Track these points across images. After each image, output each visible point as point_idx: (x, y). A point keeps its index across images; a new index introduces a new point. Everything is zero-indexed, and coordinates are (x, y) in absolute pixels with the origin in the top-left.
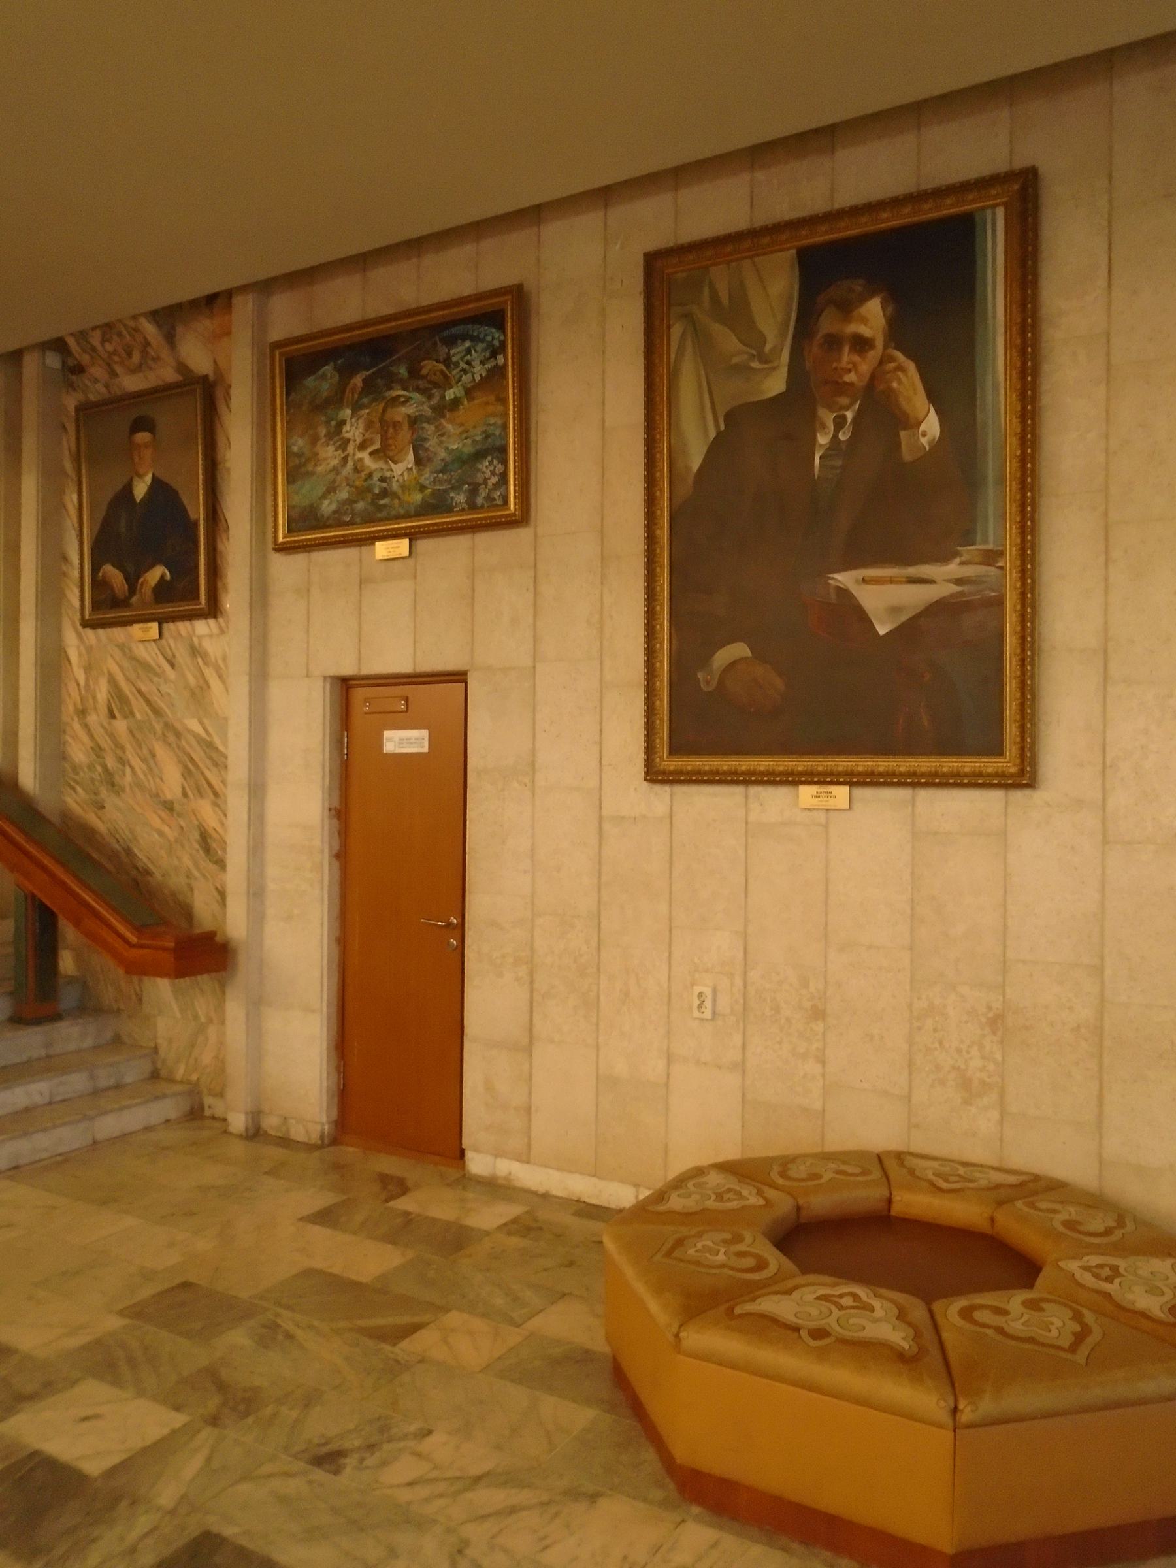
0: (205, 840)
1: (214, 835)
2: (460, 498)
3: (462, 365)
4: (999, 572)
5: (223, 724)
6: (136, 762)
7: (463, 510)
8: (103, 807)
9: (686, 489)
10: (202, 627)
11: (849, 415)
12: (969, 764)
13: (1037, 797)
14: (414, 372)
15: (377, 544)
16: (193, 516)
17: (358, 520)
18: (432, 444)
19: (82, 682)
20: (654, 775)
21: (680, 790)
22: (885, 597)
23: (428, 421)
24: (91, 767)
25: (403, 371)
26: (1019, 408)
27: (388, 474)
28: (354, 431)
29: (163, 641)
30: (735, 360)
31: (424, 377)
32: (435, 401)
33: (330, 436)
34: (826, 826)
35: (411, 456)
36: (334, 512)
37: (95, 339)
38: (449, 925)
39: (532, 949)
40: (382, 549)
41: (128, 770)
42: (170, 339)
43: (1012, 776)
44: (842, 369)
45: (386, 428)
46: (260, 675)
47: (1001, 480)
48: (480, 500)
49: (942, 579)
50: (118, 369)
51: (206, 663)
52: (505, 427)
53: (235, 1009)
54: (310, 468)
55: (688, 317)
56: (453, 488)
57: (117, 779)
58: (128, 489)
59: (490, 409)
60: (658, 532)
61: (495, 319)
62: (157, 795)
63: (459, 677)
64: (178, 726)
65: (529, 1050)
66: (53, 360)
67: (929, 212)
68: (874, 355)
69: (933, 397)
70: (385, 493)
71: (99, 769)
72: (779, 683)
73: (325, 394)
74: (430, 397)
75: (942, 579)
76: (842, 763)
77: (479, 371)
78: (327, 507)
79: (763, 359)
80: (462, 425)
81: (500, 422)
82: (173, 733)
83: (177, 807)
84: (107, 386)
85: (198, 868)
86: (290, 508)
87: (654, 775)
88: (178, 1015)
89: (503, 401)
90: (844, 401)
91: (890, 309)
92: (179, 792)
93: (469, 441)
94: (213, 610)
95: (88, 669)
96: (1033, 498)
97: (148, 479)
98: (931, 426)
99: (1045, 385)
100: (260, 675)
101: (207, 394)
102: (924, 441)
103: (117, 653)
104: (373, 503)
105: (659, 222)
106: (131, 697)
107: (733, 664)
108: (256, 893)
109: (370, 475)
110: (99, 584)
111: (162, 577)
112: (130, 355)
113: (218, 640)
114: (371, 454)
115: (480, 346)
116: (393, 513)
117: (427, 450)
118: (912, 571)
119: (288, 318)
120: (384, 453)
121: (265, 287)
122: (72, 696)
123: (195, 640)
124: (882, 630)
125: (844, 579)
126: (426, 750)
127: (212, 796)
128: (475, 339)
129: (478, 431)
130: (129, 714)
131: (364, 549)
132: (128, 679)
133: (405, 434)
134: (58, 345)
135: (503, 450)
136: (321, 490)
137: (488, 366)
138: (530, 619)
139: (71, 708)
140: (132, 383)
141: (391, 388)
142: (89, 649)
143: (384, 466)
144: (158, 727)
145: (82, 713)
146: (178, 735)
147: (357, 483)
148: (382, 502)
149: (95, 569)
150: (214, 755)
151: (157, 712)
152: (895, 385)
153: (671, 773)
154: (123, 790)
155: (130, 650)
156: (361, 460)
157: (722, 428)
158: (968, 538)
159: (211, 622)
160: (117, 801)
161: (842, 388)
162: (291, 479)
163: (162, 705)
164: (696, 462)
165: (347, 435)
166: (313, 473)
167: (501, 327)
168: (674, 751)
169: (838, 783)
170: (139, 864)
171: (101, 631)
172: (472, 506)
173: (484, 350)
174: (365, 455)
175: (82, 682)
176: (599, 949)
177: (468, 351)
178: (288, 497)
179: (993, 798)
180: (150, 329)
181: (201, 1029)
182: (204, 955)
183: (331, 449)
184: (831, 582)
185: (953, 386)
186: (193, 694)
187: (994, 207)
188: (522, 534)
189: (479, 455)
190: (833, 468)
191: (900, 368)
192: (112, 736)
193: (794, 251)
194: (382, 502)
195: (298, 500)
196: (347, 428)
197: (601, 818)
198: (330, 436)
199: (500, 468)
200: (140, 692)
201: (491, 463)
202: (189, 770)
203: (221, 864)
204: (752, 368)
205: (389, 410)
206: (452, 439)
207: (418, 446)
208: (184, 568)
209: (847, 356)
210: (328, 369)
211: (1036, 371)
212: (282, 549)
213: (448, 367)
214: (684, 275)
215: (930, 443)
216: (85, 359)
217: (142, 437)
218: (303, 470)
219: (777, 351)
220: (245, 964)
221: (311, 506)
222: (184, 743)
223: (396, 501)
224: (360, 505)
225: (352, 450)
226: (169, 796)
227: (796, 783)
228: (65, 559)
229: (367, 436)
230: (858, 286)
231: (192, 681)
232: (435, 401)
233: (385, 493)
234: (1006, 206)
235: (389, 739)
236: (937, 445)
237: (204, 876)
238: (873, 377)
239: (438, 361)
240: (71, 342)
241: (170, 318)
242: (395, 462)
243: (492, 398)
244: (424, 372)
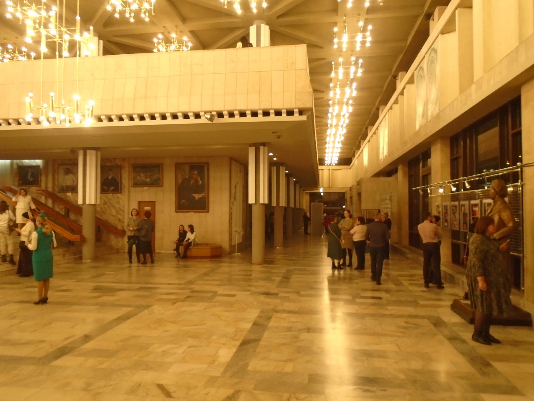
0: (119, 220)
5: (124, 206)
10: (119, 195)
20: (176, 212)
22: (197, 196)
28: (142, 175)
40: (145, 188)
46: (129, 201)
49: (201, 195)
63: (154, 202)
75: (201, 195)
82: (114, 207)
87: (176, 212)
98: (201, 182)
100: (129, 201)
120: (146, 178)
125: (193, 195)
130: (107, 204)
162: (133, 179)
164: (180, 182)
179: (206, 213)
185: (202, 179)
202: (117, 211)
207: (150, 178)
225: (142, 177)
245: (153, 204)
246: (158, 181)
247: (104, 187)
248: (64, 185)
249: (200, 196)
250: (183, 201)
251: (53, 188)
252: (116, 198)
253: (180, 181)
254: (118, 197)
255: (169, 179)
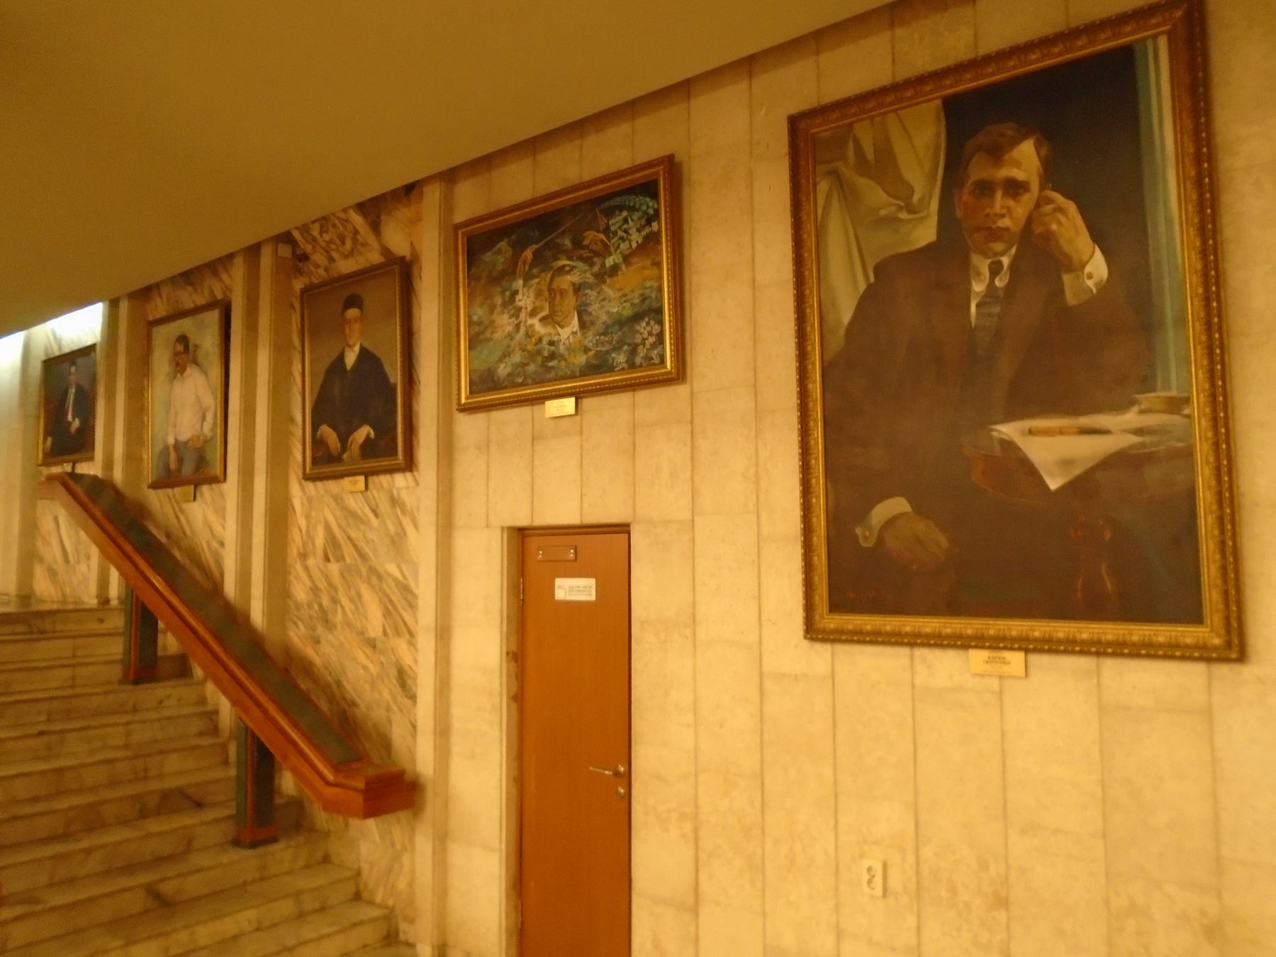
1: (410, 672)
2: (621, 358)
3: (620, 233)
4: (1186, 420)
6: (345, 601)
7: (623, 369)
8: (319, 642)
9: (837, 341)
10: (400, 480)
11: (1006, 261)
12: (1162, 633)
13: (1247, 672)
14: (578, 244)
15: (548, 403)
16: (392, 380)
17: (529, 381)
18: (594, 308)
19: (304, 529)
20: (812, 631)
21: (841, 649)
22: (1055, 449)
23: (591, 287)
24: (310, 606)
25: (567, 242)
26: (1198, 243)
27: (555, 338)
28: (525, 300)
29: (369, 493)
30: (883, 212)
31: (586, 247)
32: (596, 269)
33: (504, 305)
34: (1001, 693)
35: (576, 321)
36: (509, 375)
37: (315, 231)
38: (617, 774)
39: (697, 807)
41: (339, 610)
42: (376, 227)
43: (1215, 648)
44: (996, 215)
45: (553, 294)
47: (1181, 321)
48: (638, 360)
49: (1119, 429)
50: (334, 254)
51: (404, 513)
52: (660, 290)
53: (424, 844)
54: (488, 335)
55: (835, 174)
56: (614, 349)
57: (330, 616)
58: (341, 358)
59: (647, 273)
60: (810, 386)
61: (648, 188)
62: (362, 633)
64: (381, 570)
65: (694, 908)
66: (284, 251)
67: (1082, 49)
68: (1028, 199)
69: (1098, 237)
70: (552, 356)
71: (316, 607)
72: (943, 541)
73: (500, 267)
74: (592, 265)
75: (1119, 429)
76: (1016, 627)
77: (636, 238)
78: (503, 370)
79: (911, 209)
80: (621, 289)
81: (655, 284)
82: (375, 574)
83: (379, 645)
84: (326, 270)
85: (395, 702)
86: (471, 372)
88: (378, 840)
89: (658, 265)
90: (999, 246)
91: (1044, 152)
92: (380, 630)
93: (628, 304)
94: (409, 465)
95: (308, 517)
96: (1221, 338)
97: (357, 349)
98: (1097, 267)
99: (1227, 219)
101: (403, 272)
102: (1090, 283)
103: (333, 504)
104: (543, 365)
105: (801, 86)
106: (343, 544)
107: (891, 522)
108: (443, 731)
109: (540, 339)
110: (318, 443)
111: (368, 437)
112: (343, 243)
113: (414, 490)
114: (541, 320)
115: (636, 215)
116: (561, 373)
117: (590, 314)
118: (1084, 421)
119: (471, 201)
121: (450, 177)
122: (296, 539)
123: (395, 492)
124: (1053, 484)
125: (1008, 430)
126: (593, 598)
127: (407, 636)
128: (632, 209)
129: (636, 294)
130: (341, 559)
131: (536, 407)
132: (340, 527)
133: (570, 301)
134: (286, 238)
135: (659, 311)
136: (498, 354)
137: (644, 233)
138: (688, 474)
139: (295, 551)
140: (346, 266)
141: (557, 259)
142: (310, 500)
143: (552, 331)
144: (364, 570)
145: (303, 556)
146: (380, 577)
147: (529, 348)
148: (551, 364)
149: (315, 428)
150: (409, 597)
151: (363, 556)
152: (1054, 227)
153: (832, 632)
154: (335, 627)
155: (342, 499)
156: (532, 326)
157: (872, 280)
158: (1147, 383)
159: (408, 475)
160: (330, 637)
161: (996, 234)
162: (471, 346)
163: (367, 550)
164: (846, 315)
165: (521, 304)
166: (491, 339)
167: (655, 196)
168: (835, 607)
169: (1012, 649)
170: (347, 696)
171: (319, 484)
172: (632, 366)
173: (640, 219)
174: (535, 321)
175: (304, 529)
176: (763, 811)
177: (626, 221)
178: (470, 361)
179: (1193, 673)
180: (357, 219)
181: (397, 857)
182: (394, 792)
183: (506, 317)
184: (994, 434)
186: (393, 542)
187: (1155, 37)
188: (680, 392)
189: (637, 318)
190: (990, 315)
191: (1060, 210)
192: (327, 577)
193: (939, 102)
194: (551, 364)
195: (477, 365)
196: (519, 297)
197: (761, 675)
198: (504, 305)
199: (656, 328)
200: (349, 538)
201: (648, 324)
202: (389, 611)
203: (413, 698)
204: (900, 220)
205: (557, 279)
206: (610, 303)
207: (582, 312)
208: (385, 429)
209: (1000, 201)
210: (503, 244)
211: (1214, 204)
212: (464, 409)
213: (608, 237)
214: (828, 134)
215: (1096, 285)
216: (308, 248)
217: (353, 313)
218: (482, 337)
219: (924, 201)
220: (431, 797)
221: (489, 370)
222: (385, 586)
223: (563, 363)
224: (532, 368)
226: (372, 634)
227: (965, 647)
228: (292, 420)
229: (538, 304)
230: (1009, 129)
231: (392, 529)
232: (596, 269)
233: (552, 356)
234: (1169, 33)
235: (560, 587)
236: (1104, 288)
237: (401, 710)
238: (1030, 220)
239: (598, 231)
240: (296, 234)
241: (374, 209)
242: (562, 327)
243: (648, 263)
244: (586, 242)
245: (604, 544)
246: (644, 328)
247: (325, 430)
248: (171, 441)
249: (1088, 449)
250: (883, 511)
251: (132, 458)
252: (384, 507)
253: (844, 292)
254: (395, 502)
255: (743, 293)
